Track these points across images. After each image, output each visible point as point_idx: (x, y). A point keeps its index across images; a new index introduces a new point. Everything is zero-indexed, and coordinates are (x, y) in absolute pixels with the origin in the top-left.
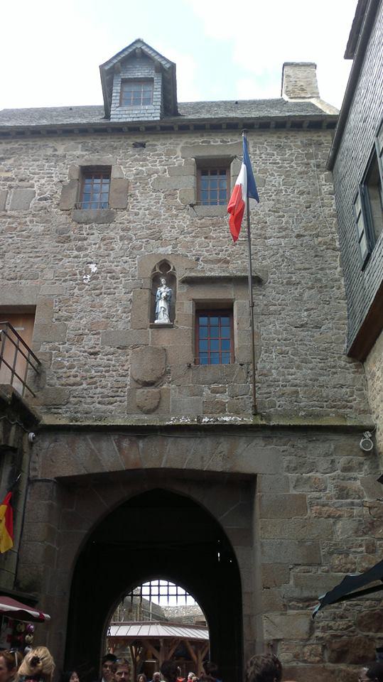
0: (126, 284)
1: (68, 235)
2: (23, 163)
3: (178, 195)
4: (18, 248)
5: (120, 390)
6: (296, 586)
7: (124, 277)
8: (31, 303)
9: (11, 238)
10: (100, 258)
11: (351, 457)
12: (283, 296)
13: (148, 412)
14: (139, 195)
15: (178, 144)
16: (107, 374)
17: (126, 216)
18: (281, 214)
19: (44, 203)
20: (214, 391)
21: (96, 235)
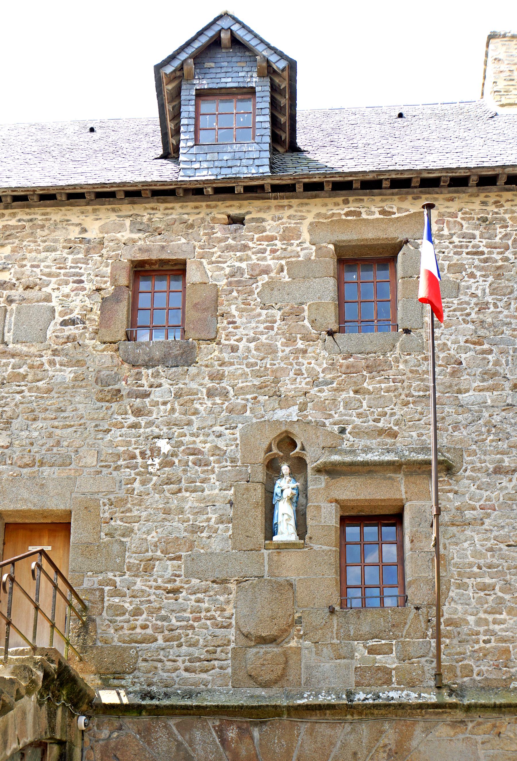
0: (221, 474)
1: (117, 387)
2: (28, 255)
3: (306, 314)
4: (33, 411)
5: (219, 649)
7: (218, 462)
8: (62, 507)
10: (175, 428)
12: (488, 493)
13: (265, 685)
15: (303, 218)
16: (196, 624)
17: (216, 353)
18: (486, 346)
19: (70, 330)
20: (372, 651)
21: (166, 386)
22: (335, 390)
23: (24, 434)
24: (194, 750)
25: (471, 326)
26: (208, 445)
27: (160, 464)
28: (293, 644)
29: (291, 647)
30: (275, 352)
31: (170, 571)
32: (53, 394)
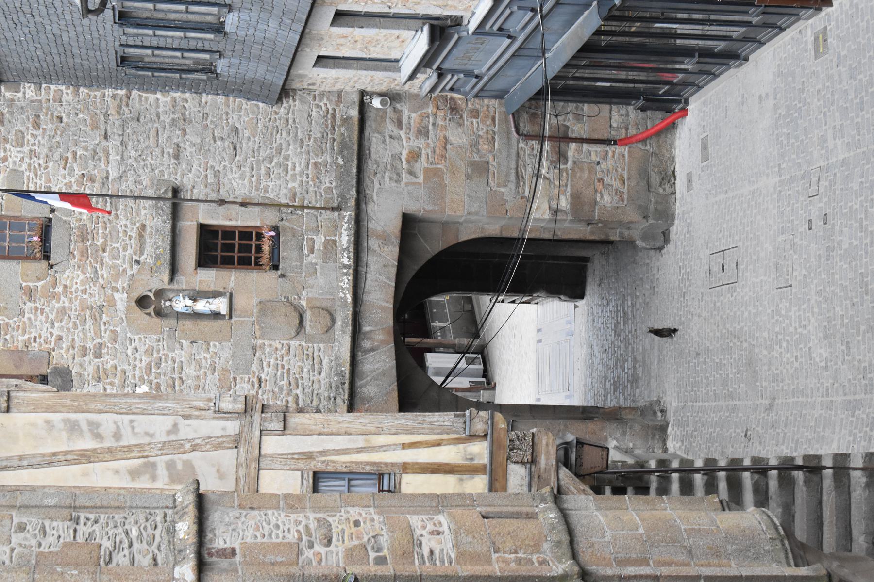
5: (306, 352)
10: (127, 382)
12: (194, 165)
13: (333, 321)
14: (27, 336)
16: (286, 367)
17: (62, 351)
18: (70, 155)
20: (312, 251)
22: (102, 266)
24: (378, 369)
25: (51, 164)
26: (143, 358)
28: (304, 303)
29: (307, 304)
30: (64, 308)
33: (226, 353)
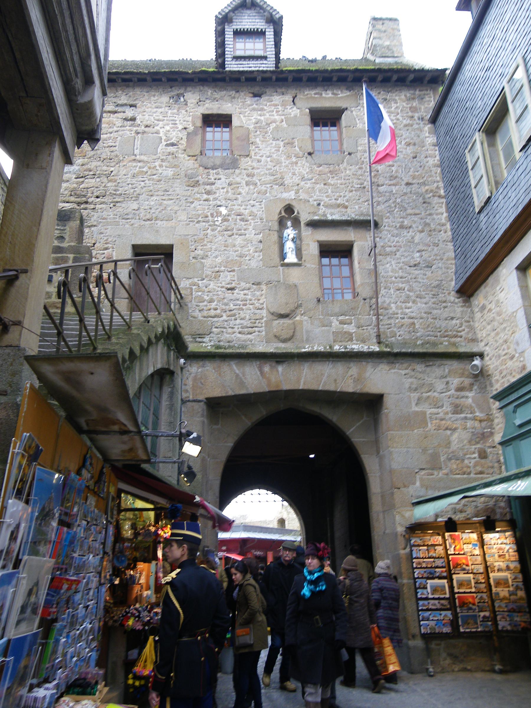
0: (255, 226)
1: (197, 179)
2: (147, 110)
3: (296, 143)
4: (151, 191)
5: (258, 321)
6: (422, 486)
7: (253, 219)
8: (168, 243)
9: (143, 181)
10: (229, 201)
11: (462, 379)
13: (284, 341)
16: (244, 307)
17: (250, 163)
20: (342, 323)
21: (223, 179)
23: (147, 203)
24: (246, 378)
26: (247, 211)
27: (222, 220)
28: (298, 318)
31: (229, 278)
32: (162, 182)
33: (254, 264)
